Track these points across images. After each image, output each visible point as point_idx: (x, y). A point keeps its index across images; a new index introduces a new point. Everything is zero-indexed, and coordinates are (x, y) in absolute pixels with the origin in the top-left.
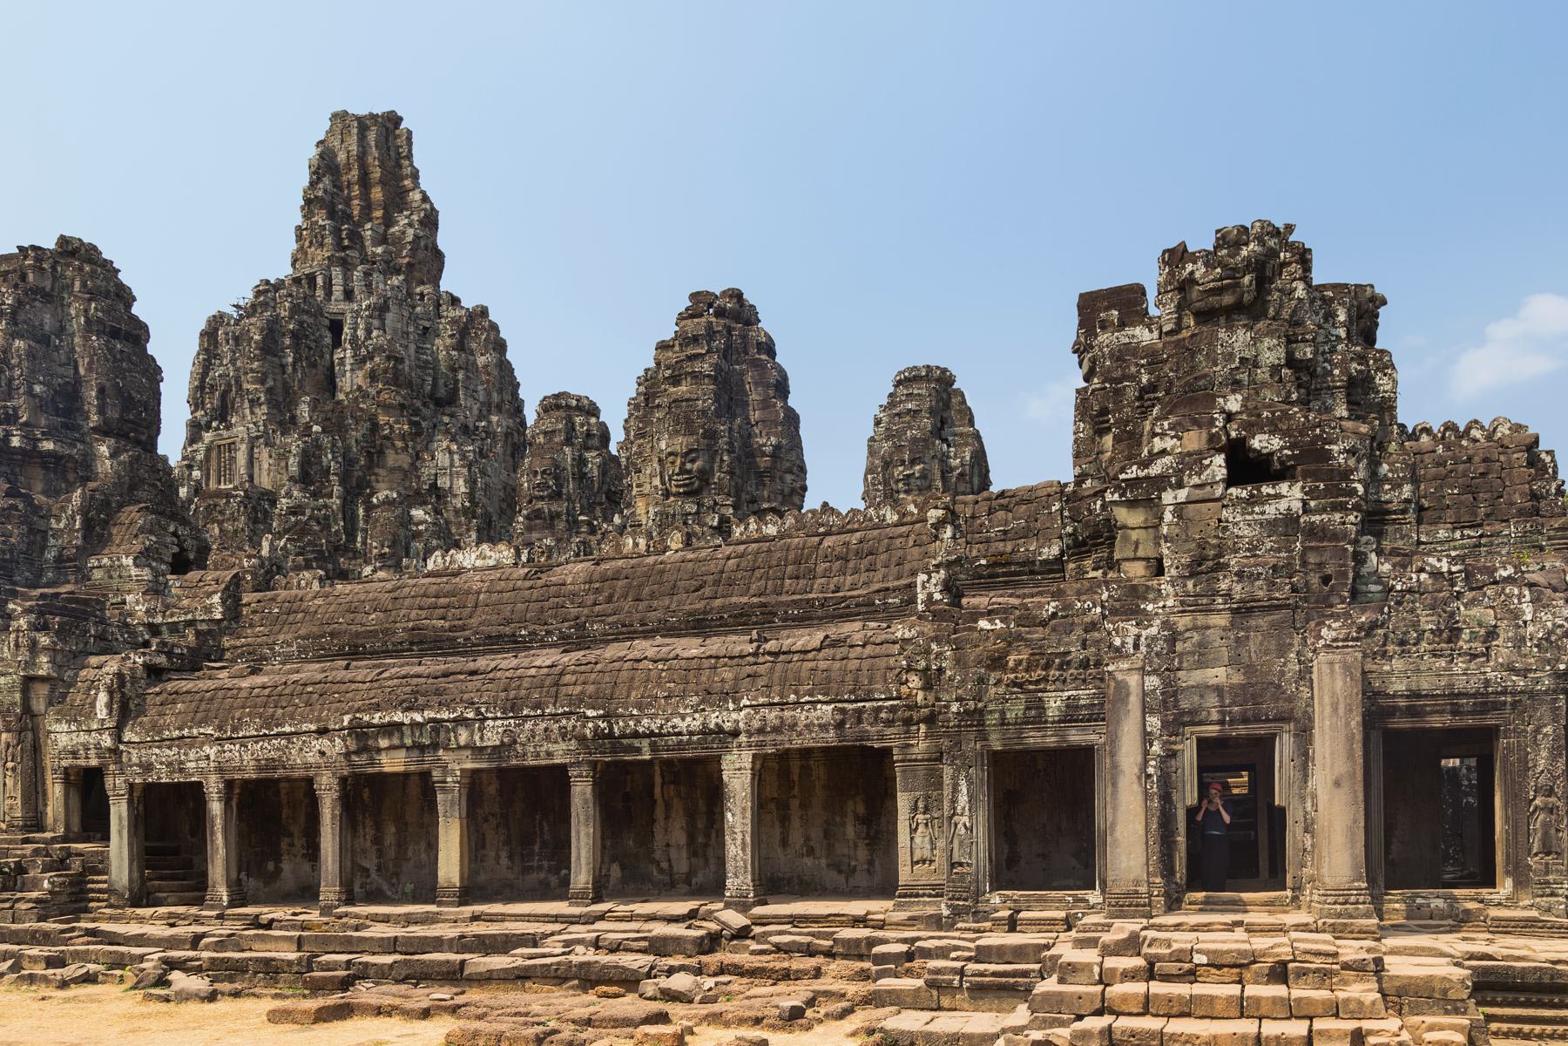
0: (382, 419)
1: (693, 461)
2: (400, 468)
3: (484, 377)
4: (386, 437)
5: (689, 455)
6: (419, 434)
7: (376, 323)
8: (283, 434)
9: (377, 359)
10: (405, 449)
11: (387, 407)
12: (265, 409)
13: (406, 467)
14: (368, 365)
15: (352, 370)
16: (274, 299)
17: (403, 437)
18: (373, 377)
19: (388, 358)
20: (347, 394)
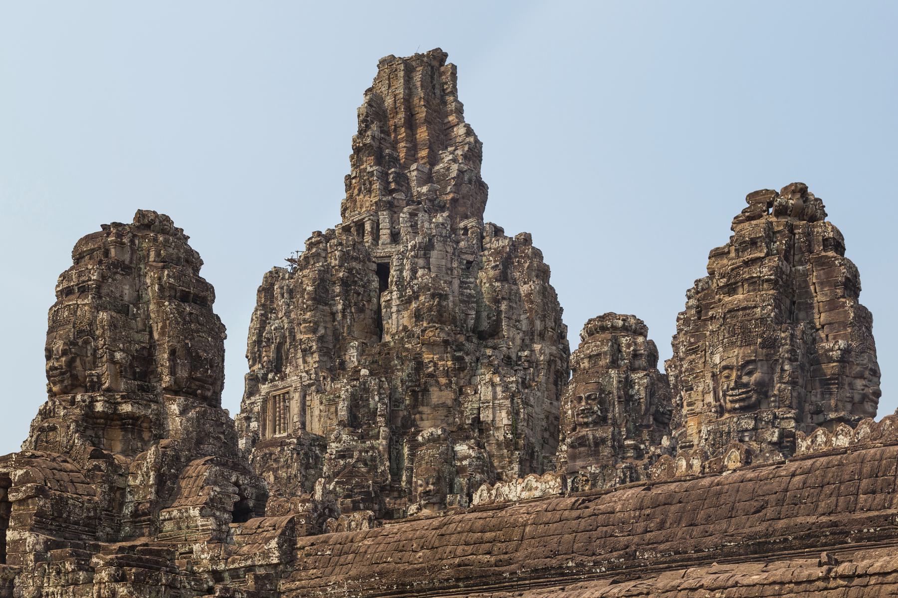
0: (427, 357)
1: (750, 373)
2: (444, 405)
3: (527, 306)
4: (431, 375)
5: (746, 366)
6: (462, 369)
7: (421, 262)
8: (333, 380)
9: (422, 298)
10: (449, 385)
11: (430, 345)
12: (316, 357)
13: (449, 402)
14: (414, 305)
15: (398, 311)
16: (325, 250)
17: (447, 374)
18: (418, 316)
19: (433, 296)
20: (393, 336)
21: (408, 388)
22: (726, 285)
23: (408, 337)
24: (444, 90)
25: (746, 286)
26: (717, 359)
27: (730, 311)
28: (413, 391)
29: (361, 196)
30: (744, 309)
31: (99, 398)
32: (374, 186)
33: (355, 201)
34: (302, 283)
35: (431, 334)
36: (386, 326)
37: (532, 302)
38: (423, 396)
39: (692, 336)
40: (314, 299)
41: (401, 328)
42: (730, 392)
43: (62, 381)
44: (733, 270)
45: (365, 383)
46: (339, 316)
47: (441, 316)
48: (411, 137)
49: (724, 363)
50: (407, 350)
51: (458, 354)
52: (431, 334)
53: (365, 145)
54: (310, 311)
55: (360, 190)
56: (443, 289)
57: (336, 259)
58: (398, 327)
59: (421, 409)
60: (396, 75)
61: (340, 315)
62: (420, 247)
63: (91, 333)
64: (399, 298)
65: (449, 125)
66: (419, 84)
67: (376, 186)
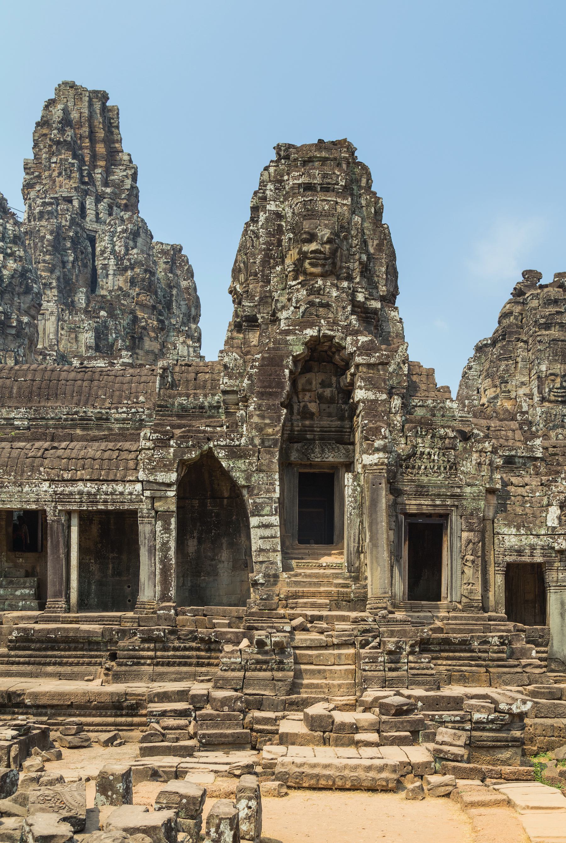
0: (140, 314)
2: (152, 352)
3: (186, 296)
4: (144, 328)
6: (162, 329)
7: (131, 243)
8: (70, 313)
9: (137, 270)
10: (156, 338)
11: (143, 306)
12: (55, 292)
13: (156, 351)
14: (129, 273)
15: (114, 275)
17: (154, 330)
18: (133, 282)
19: (146, 271)
20: (110, 292)
21: (128, 333)
22: (545, 323)
23: (124, 296)
24: (111, 123)
25: (557, 327)
26: (543, 368)
27: (553, 340)
28: (133, 337)
30: (562, 341)
31: (360, 290)
32: (73, 175)
33: (54, 181)
34: (39, 231)
35: (144, 298)
36: (101, 283)
37: (190, 294)
38: (139, 341)
39: (502, 349)
40: (53, 246)
41: (116, 287)
42: (555, 390)
43: (323, 265)
44: (550, 315)
45: (106, 322)
47: (150, 287)
48: (92, 148)
49: (549, 372)
51: (161, 318)
52: (144, 298)
53: (65, 141)
54: (50, 255)
55: (60, 174)
56: (152, 268)
57: (66, 221)
58: (113, 286)
59: (137, 351)
60: (81, 98)
61: (70, 265)
62: (131, 232)
63: (348, 231)
64: (116, 265)
65: (115, 150)
66: (98, 111)
67: (76, 175)
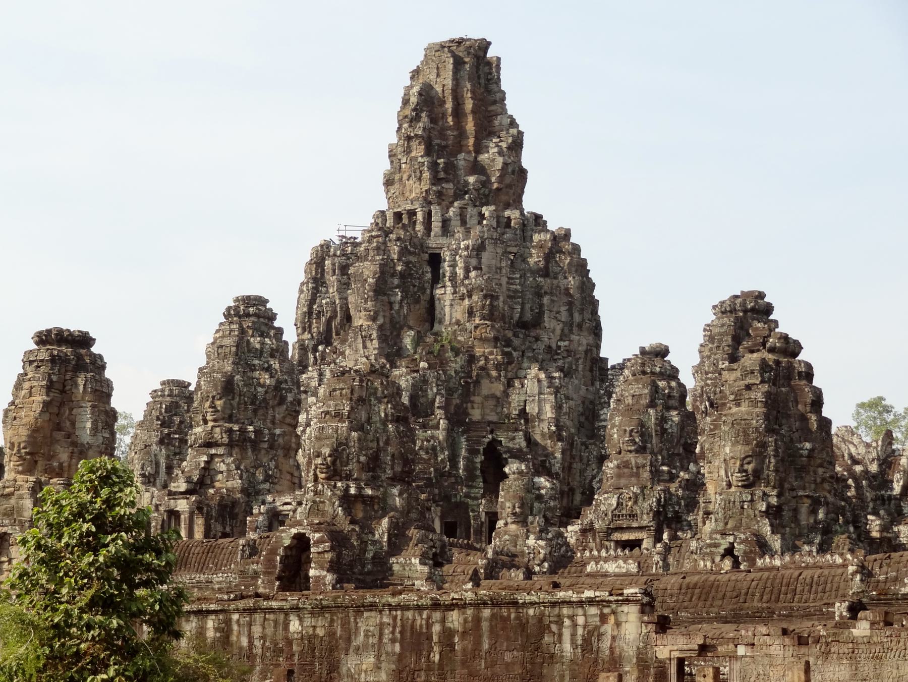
0: (478, 351)
2: (493, 396)
4: (482, 368)
6: (510, 363)
7: (474, 262)
9: (475, 298)
11: (483, 340)
12: (376, 343)
13: (498, 394)
14: (467, 302)
18: (471, 313)
29: (411, 182)
38: (474, 387)
40: (375, 291)
41: (454, 320)
45: (424, 375)
46: (396, 307)
47: (493, 314)
50: (459, 342)
51: (506, 349)
55: (410, 176)
58: (451, 320)
62: (473, 248)
65: (493, 113)
67: (426, 175)
